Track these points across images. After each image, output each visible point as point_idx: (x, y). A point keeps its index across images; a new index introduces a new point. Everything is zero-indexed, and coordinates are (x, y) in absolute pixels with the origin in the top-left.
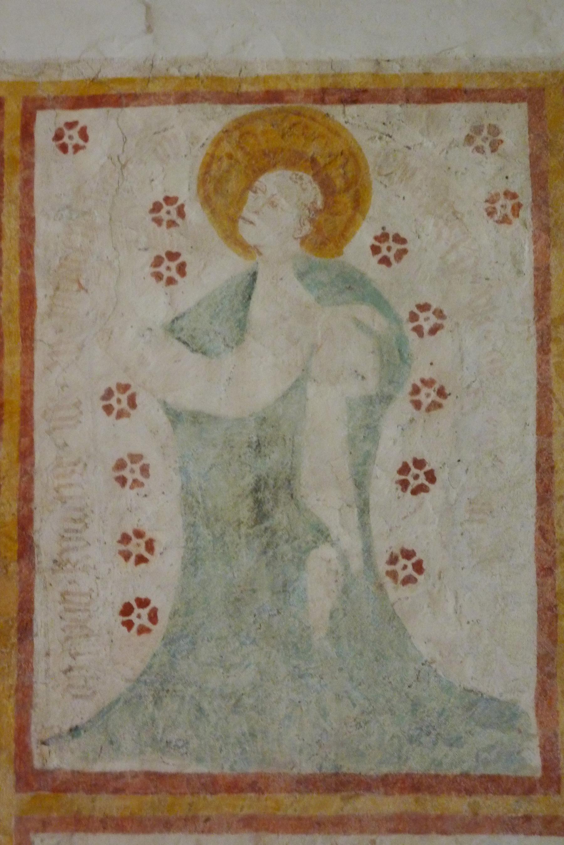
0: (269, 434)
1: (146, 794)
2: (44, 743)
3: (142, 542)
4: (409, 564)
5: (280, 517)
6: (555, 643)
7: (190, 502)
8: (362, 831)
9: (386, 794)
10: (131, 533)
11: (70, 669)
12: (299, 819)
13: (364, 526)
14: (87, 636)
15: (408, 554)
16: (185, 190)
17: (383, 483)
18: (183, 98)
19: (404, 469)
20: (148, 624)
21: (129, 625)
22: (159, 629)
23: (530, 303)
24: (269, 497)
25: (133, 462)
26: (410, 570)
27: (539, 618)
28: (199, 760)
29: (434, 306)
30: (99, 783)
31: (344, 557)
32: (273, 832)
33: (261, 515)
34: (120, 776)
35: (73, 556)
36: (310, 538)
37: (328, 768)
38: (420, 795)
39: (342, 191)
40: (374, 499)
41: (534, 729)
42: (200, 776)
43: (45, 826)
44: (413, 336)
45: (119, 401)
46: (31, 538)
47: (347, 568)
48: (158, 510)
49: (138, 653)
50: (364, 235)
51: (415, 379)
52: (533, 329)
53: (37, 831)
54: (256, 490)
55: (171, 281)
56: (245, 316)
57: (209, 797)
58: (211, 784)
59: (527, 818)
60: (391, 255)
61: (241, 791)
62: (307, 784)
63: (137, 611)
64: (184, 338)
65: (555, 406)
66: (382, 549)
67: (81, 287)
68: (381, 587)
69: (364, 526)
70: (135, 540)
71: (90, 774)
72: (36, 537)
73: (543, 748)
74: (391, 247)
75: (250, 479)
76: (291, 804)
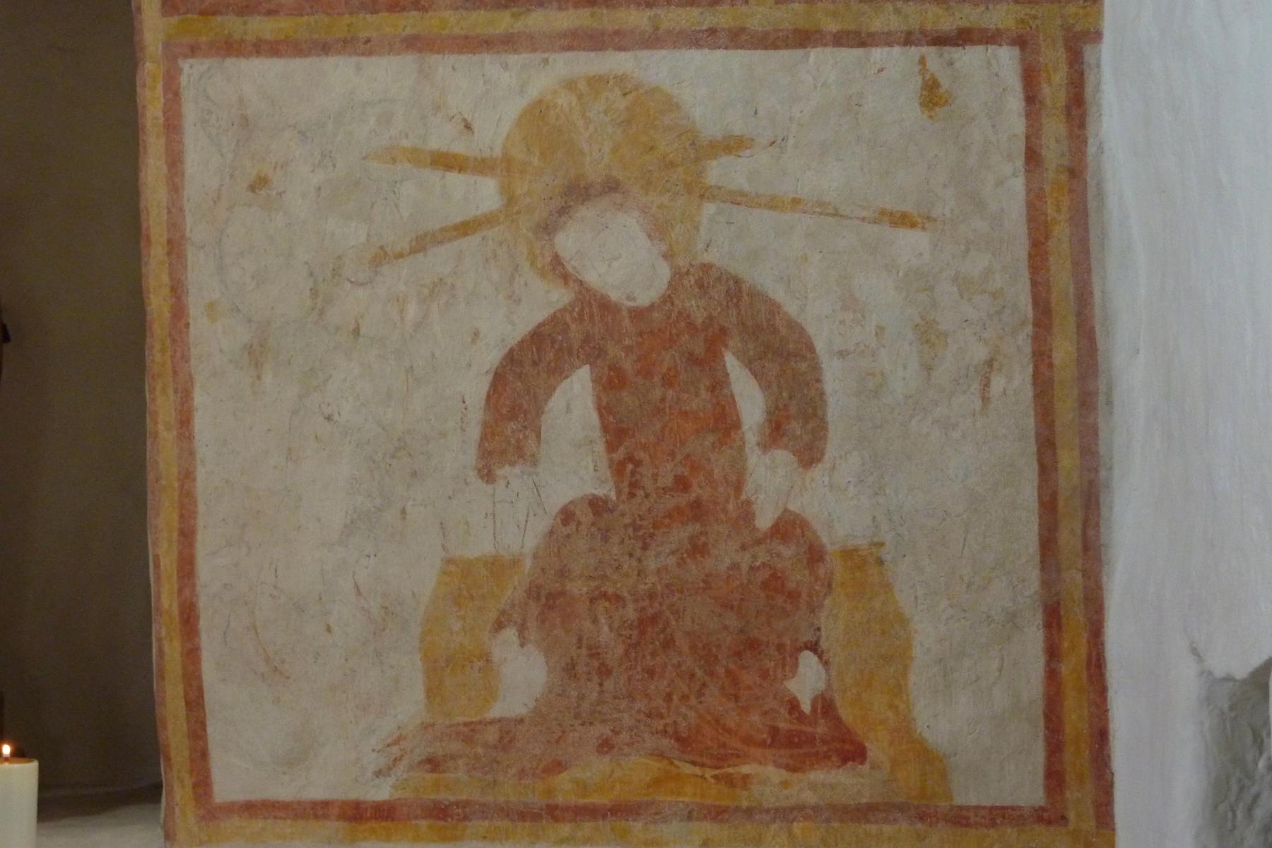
1: (302, 15)
9: (560, 9)
12: (466, 37)
32: (438, 52)
38: (596, 9)
43: (194, 51)
53: (186, 56)
57: (368, 16)
59: (712, 31)
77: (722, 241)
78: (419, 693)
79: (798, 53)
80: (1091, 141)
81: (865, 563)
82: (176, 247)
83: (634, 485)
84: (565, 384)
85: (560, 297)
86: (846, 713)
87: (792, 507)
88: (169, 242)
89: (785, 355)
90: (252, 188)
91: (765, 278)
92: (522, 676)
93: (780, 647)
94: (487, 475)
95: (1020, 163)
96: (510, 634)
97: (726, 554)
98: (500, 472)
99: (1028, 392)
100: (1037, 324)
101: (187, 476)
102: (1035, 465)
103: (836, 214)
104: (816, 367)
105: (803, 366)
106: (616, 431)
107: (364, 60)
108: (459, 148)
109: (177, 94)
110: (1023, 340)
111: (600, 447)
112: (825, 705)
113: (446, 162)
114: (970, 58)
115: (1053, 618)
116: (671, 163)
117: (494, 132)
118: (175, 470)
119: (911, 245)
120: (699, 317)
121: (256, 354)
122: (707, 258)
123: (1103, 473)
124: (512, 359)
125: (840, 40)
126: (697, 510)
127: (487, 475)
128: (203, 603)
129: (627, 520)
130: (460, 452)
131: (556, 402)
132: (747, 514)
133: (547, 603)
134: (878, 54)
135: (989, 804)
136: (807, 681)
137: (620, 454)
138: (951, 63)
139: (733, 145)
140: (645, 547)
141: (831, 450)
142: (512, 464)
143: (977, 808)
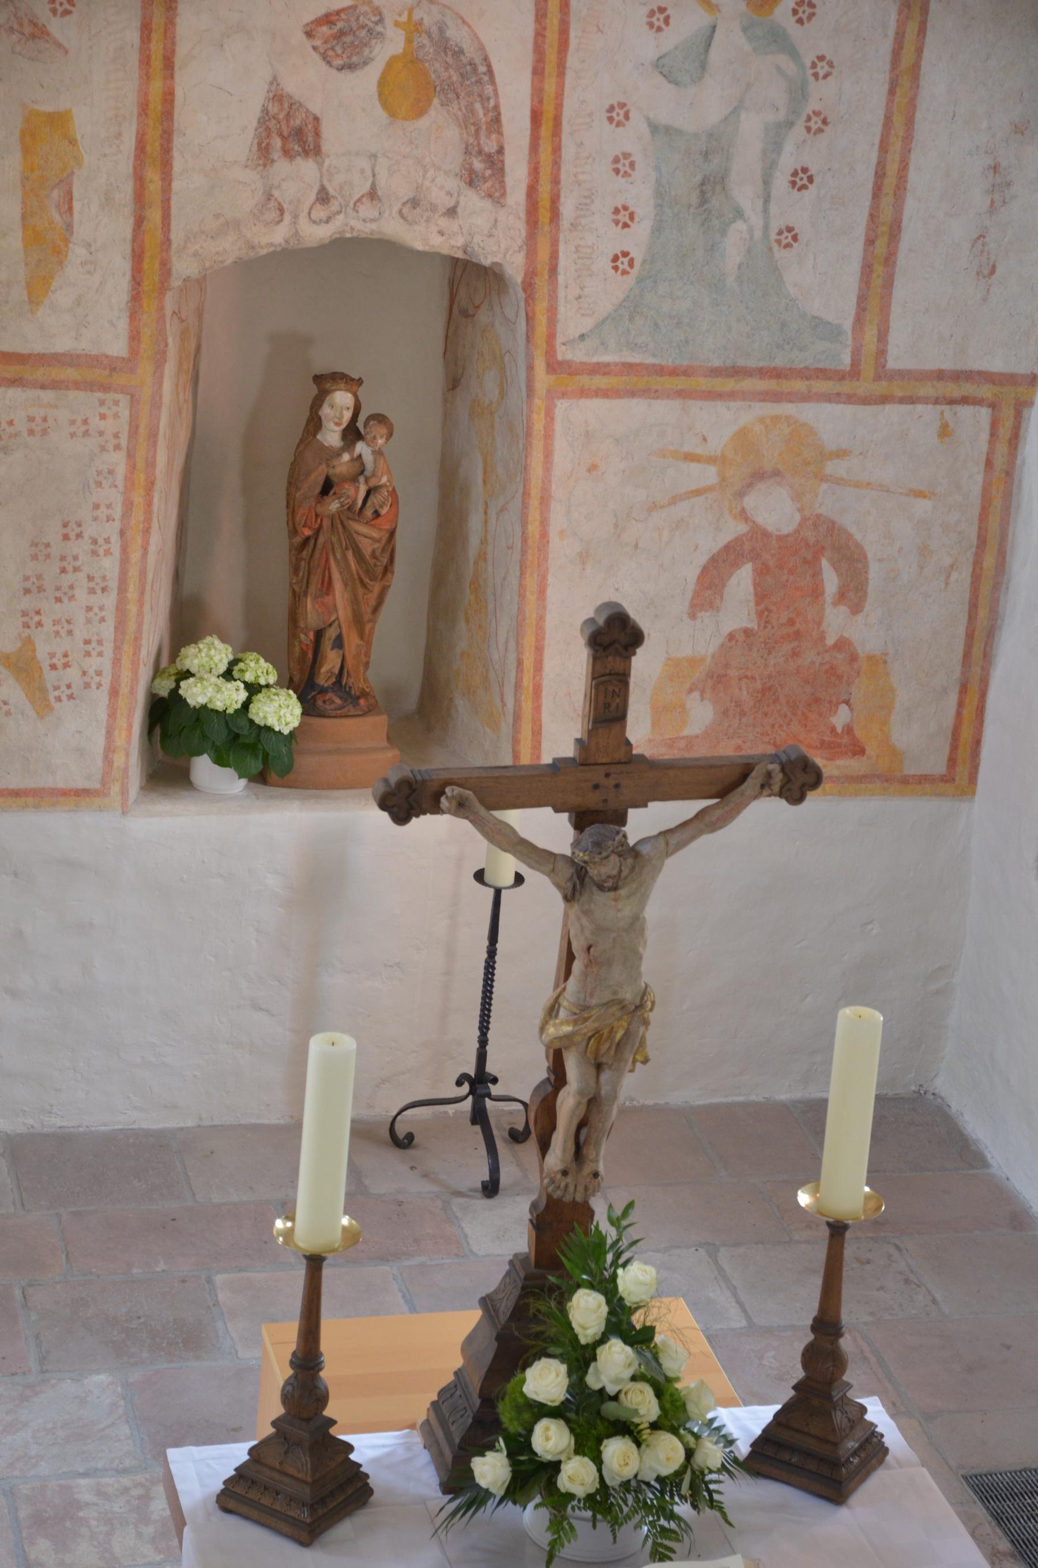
0: (714, 146)
2: (564, 344)
3: (627, 213)
4: (790, 236)
5: (715, 202)
6: (869, 288)
7: (660, 193)
8: (744, 400)
10: (620, 207)
11: (580, 297)
12: (709, 392)
13: (766, 210)
14: (591, 276)
15: (790, 229)
17: (781, 181)
19: (795, 174)
20: (628, 269)
21: (616, 268)
22: (634, 272)
23: (888, 58)
24: (711, 187)
25: (625, 158)
26: (790, 240)
27: (862, 273)
28: (654, 355)
29: (828, 58)
31: (751, 230)
33: (703, 200)
34: (608, 364)
35: (583, 221)
36: (731, 216)
37: (729, 363)
40: (774, 193)
41: (849, 342)
42: (654, 365)
43: (564, 395)
44: (812, 79)
45: (618, 115)
46: (557, 208)
47: (752, 237)
48: (639, 194)
49: (619, 287)
51: (809, 110)
52: (887, 78)
53: (559, 398)
54: (702, 184)
55: (659, 29)
56: (706, 58)
58: (660, 371)
59: (838, 394)
60: (805, 17)
61: (678, 375)
62: (716, 372)
63: (622, 259)
64: (665, 73)
65: (893, 132)
66: (775, 225)
67: (599, 30)
68: (770, 249)
69: (766, 210)
70: (622, 212)
71: (589, 364)
72: (561, 208)
73: (853, 353)
75: (699, 178)
76: (704, 383)
77: (828, 503)
78: (648, 724)
79: (881, 407)
80: (1019, 457)
81: (878, 663)
82: (545, 500)
83: (767, 622)
84: (739, 572)
85: (742, 528)
86: (858, 733)
87: (846, 635)
88: (542, 498)
89: (852, 560)
90: (589, 471)
91: (847, 522)
93: (830, 702)
94: (693, 616)
95: (982, 467)
96: (696, 694)
97: (809, 656)
98: (699, 615)
99: (969, 580)
100: (977, 548)
101: (541, 618)
102: (967, 616)
103: (888, 491)
104: (866, 566)
105: (860, 566)
106: (761, 596)
107: (653, 401)
108: (699, 451)
109: (553, 419)
110: (970, 556)
111: (752, 604)
112: (849, 730)
113: (691, 457)
114: (965, 411)
115: (964, 689)
116: (808, 461)
117: (718, 443)
118: (534, 616)
119: (922, 507)
120: (812, 541)
121: (583, 558)
122: (819, 511)
123: (999, 621)
124: (714, 560)
125: (902, 401)
126: (798, 635)
127: (693, 616)
128: (546, 684)
129: (762, 640)
131: (733, 581)
132: (822, 637)
133: (716, 680)
134: (920, 408)
135: (919, 773)
136: (841, 718)
137: (762, 607)
138: (955, 414)
139: (841, 454)
140: (770, 653)
141: (867, 607)
142: (706, 611)
143: (914, 776)
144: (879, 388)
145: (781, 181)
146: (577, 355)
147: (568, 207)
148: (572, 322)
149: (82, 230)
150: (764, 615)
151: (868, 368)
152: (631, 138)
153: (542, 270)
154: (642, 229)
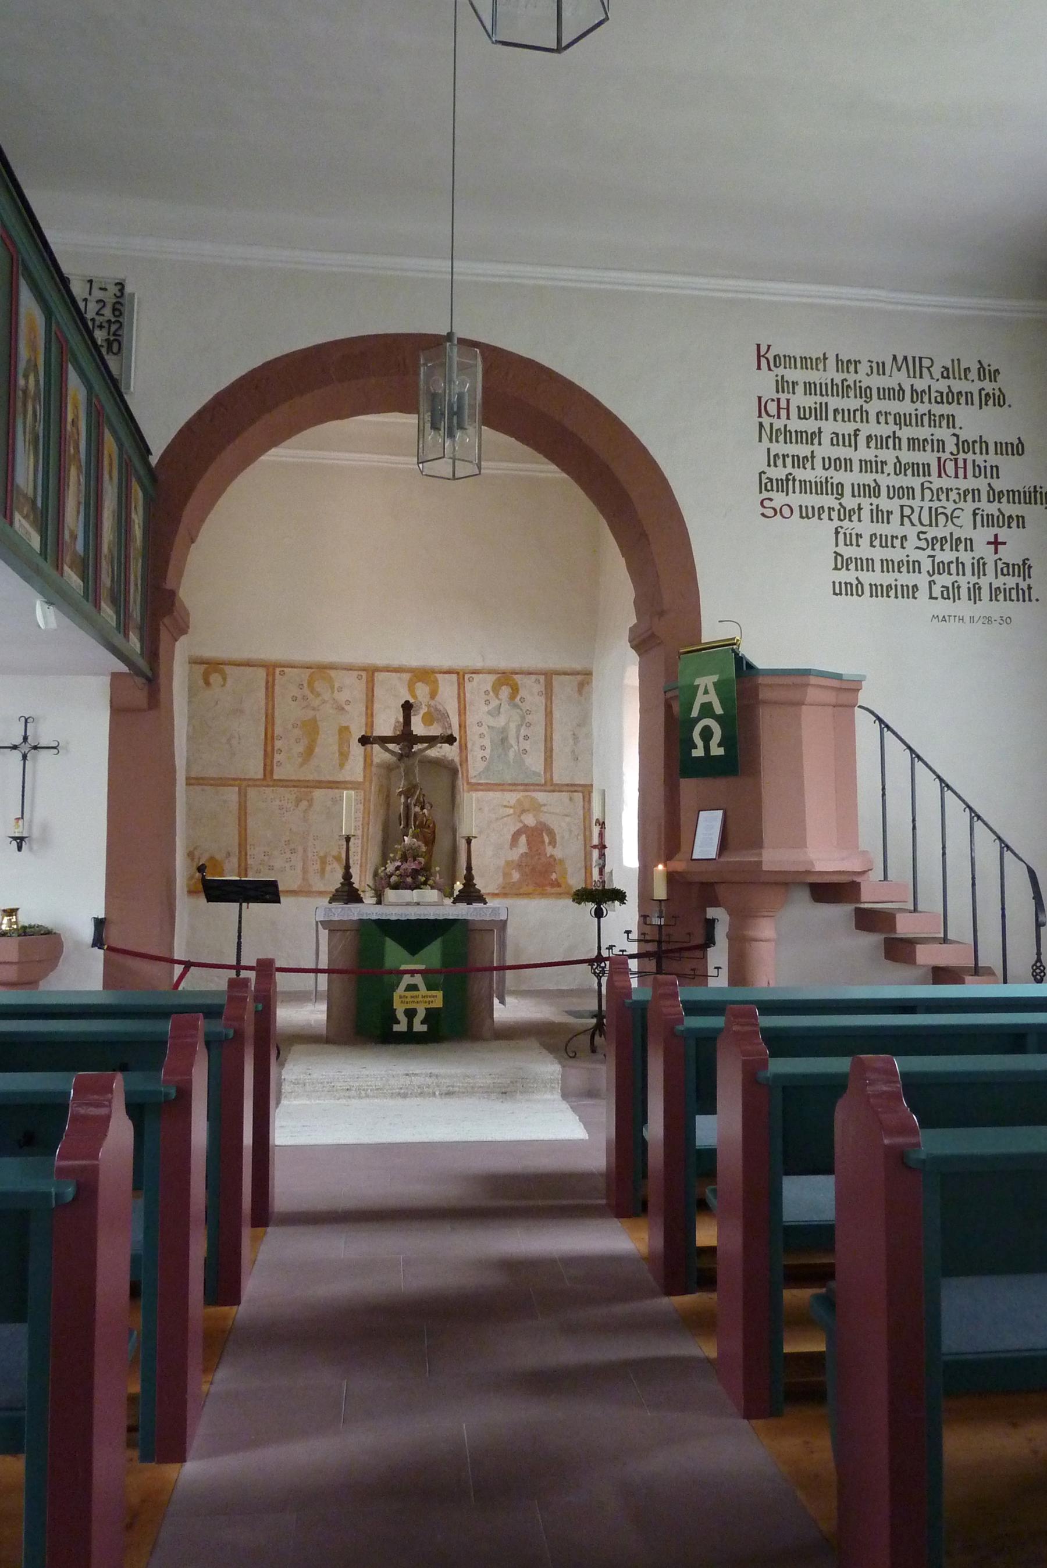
0: (504, 730)
4: (525, 751)
16: (490, 689)
17: (521, 739)
18: (490, 673)
24: (504, 740)
30: (479, 784)
39: (515, 690)
48: (487, 742)
49: (484, 764)
50: (518, 698)
62: (510, 785)
74: (522, 700)
77: (545, 818)
81: (561, 861)
89: (551, 833)
92: (516, 876)
97: (543, 859)
106: (529, 843)
112: (556, 880)
113: (505, 806)
116: (536, 808)
117: (512, 802)
119: (568, 819)
130: (507, 846)
133: (519, 866)
136: (554, 876)
139: (545, 805)
144: (552, 788)
145: (521, 739)
146: (473, 781)
147: (469, 746)
148: (472, 773)
149: (352, 752)
150: (530, 848)
151: (549, 784)
152: (484, 730)
153: (464, 761)
154: (488, 750)
